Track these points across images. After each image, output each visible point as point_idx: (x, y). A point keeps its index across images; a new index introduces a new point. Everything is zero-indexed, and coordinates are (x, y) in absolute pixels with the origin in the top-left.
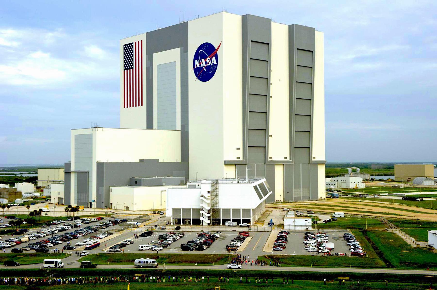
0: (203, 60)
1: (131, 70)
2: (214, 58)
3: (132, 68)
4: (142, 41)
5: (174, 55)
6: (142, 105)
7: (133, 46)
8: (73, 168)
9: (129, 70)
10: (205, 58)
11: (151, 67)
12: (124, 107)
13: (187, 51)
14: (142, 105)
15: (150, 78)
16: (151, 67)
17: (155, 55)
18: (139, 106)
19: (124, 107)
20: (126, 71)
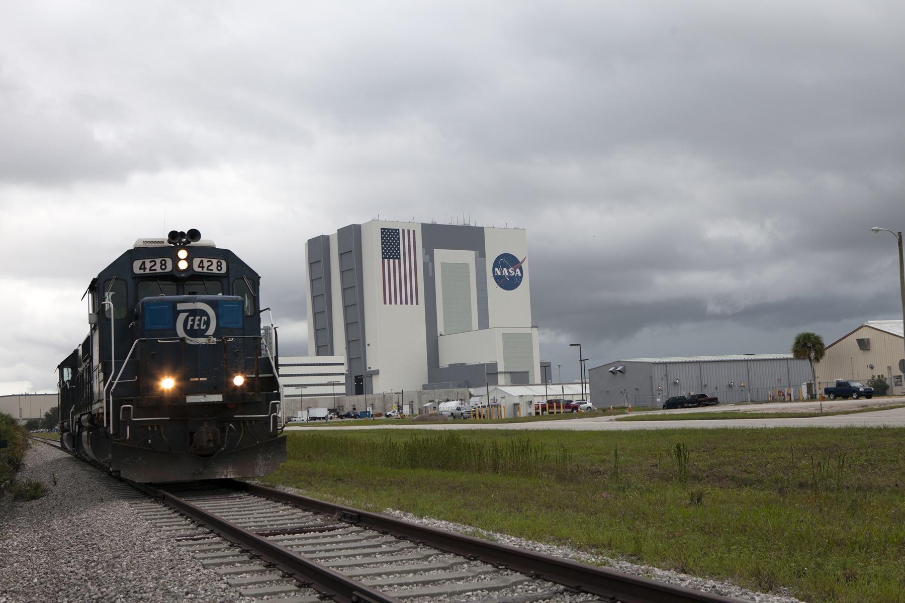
0: (505, 269)
1: (397, 261)
2: (518, 270)
3: (399, 259)
4: (414, 231)
5: (468, 257)
6: (417, 303)
7: (398, 234)
8: (501, 368)
9: (391, 261)
10: (508, 268)
11: (430, 264)
12: (385, 303)
13: (484, 256)
14: (417, 303)
15: (431, 274)
16: (430, 264)
17: (437, 252)
18: (412, 303)
19: (385, 303)
20: (386, 260)
